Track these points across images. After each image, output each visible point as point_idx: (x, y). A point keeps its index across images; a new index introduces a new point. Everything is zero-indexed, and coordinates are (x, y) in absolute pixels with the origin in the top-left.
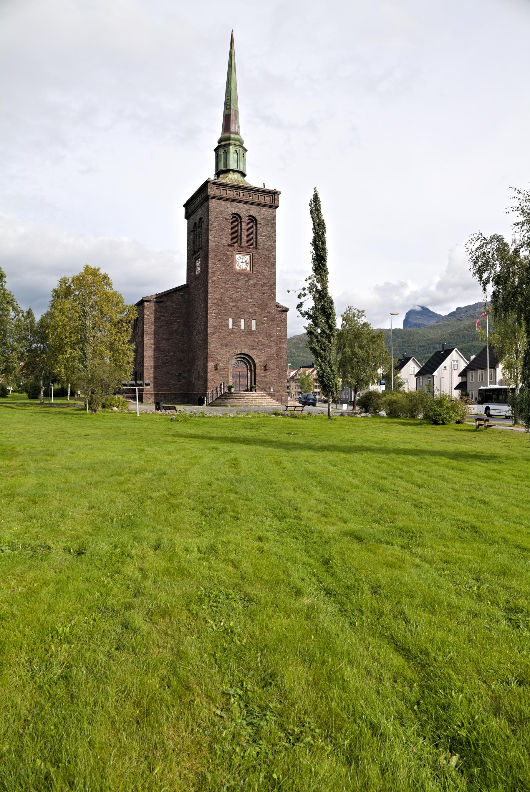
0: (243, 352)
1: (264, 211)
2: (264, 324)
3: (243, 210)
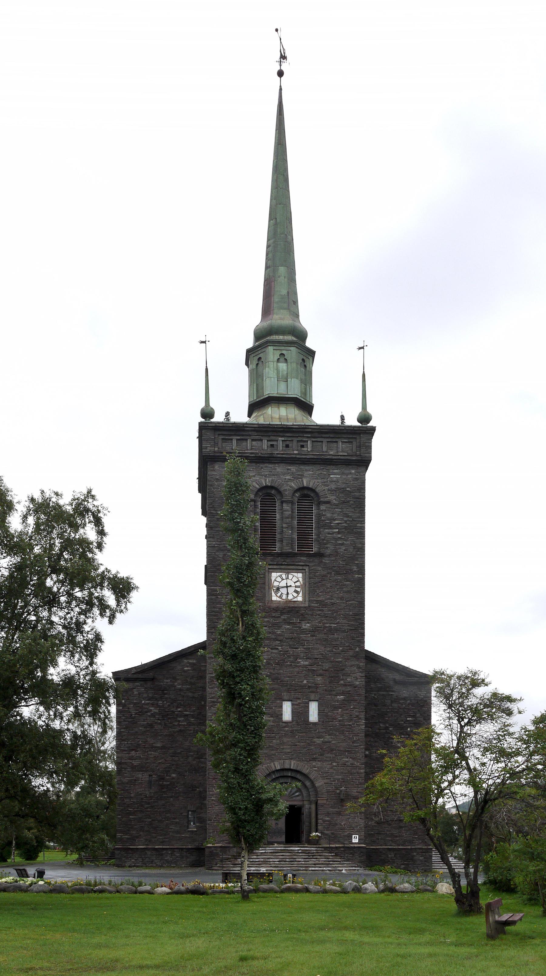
0: (287, 766)
1: (335, 475)
2: (336, 708)
3: (286, 479)
